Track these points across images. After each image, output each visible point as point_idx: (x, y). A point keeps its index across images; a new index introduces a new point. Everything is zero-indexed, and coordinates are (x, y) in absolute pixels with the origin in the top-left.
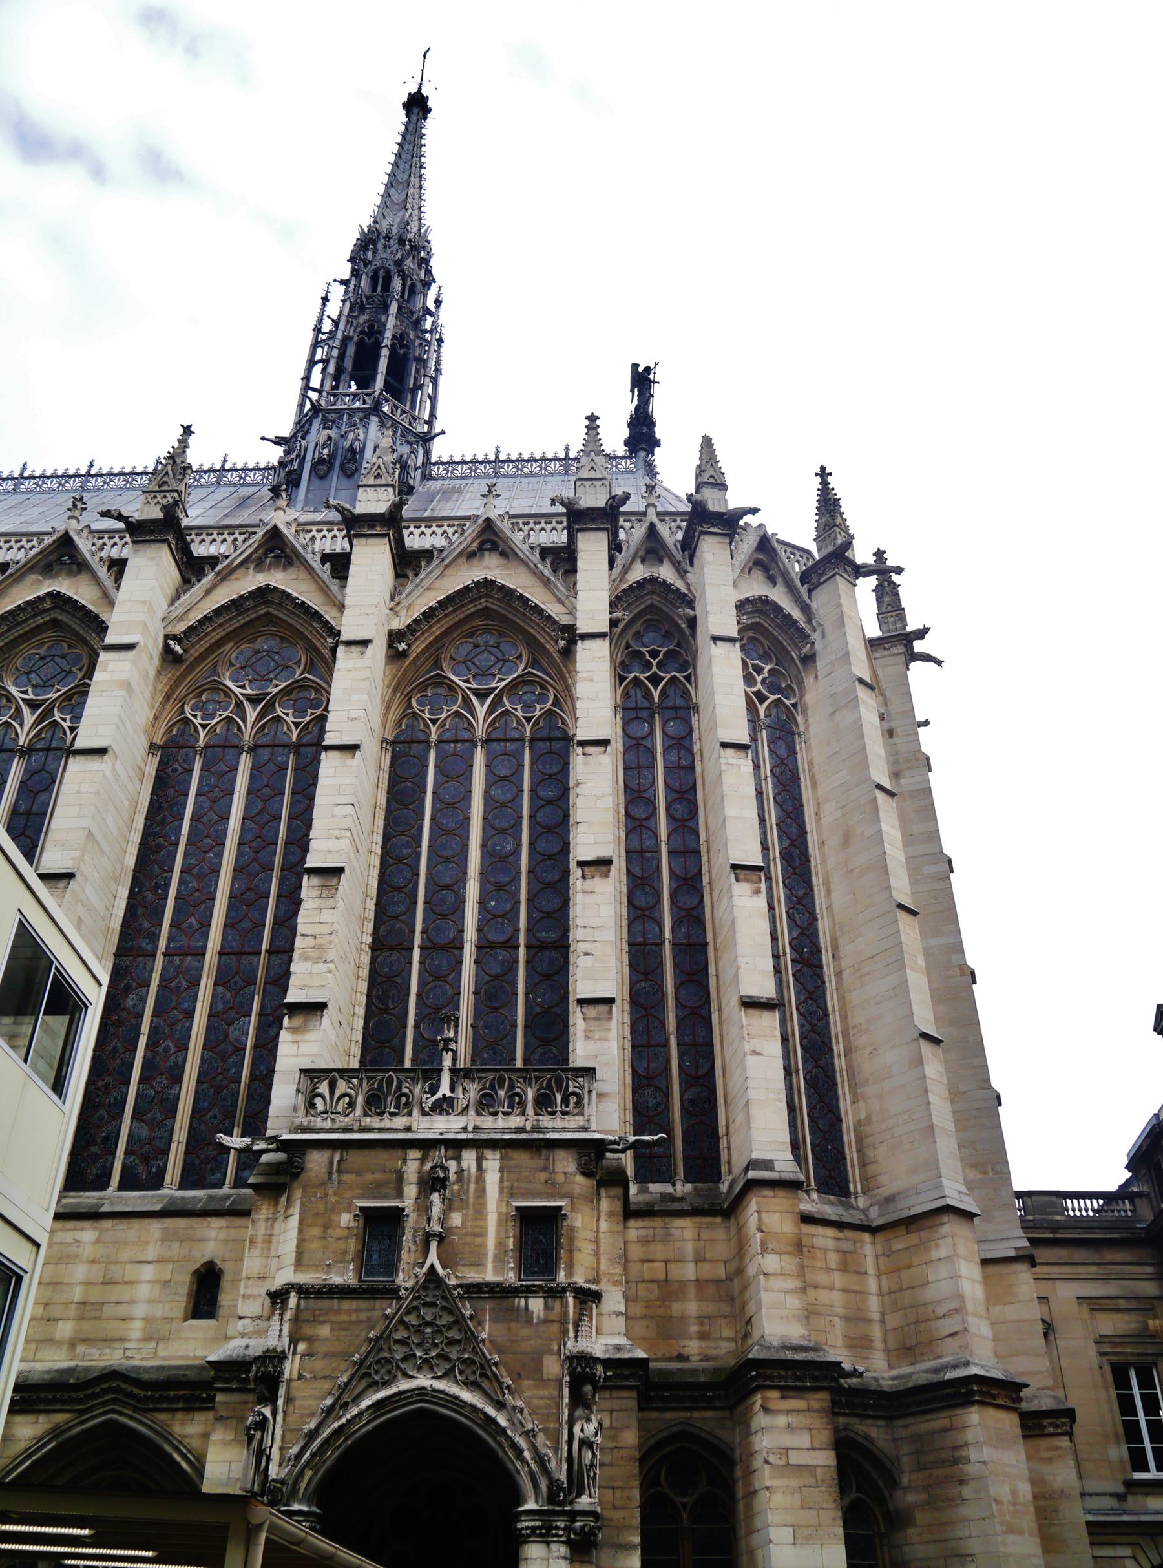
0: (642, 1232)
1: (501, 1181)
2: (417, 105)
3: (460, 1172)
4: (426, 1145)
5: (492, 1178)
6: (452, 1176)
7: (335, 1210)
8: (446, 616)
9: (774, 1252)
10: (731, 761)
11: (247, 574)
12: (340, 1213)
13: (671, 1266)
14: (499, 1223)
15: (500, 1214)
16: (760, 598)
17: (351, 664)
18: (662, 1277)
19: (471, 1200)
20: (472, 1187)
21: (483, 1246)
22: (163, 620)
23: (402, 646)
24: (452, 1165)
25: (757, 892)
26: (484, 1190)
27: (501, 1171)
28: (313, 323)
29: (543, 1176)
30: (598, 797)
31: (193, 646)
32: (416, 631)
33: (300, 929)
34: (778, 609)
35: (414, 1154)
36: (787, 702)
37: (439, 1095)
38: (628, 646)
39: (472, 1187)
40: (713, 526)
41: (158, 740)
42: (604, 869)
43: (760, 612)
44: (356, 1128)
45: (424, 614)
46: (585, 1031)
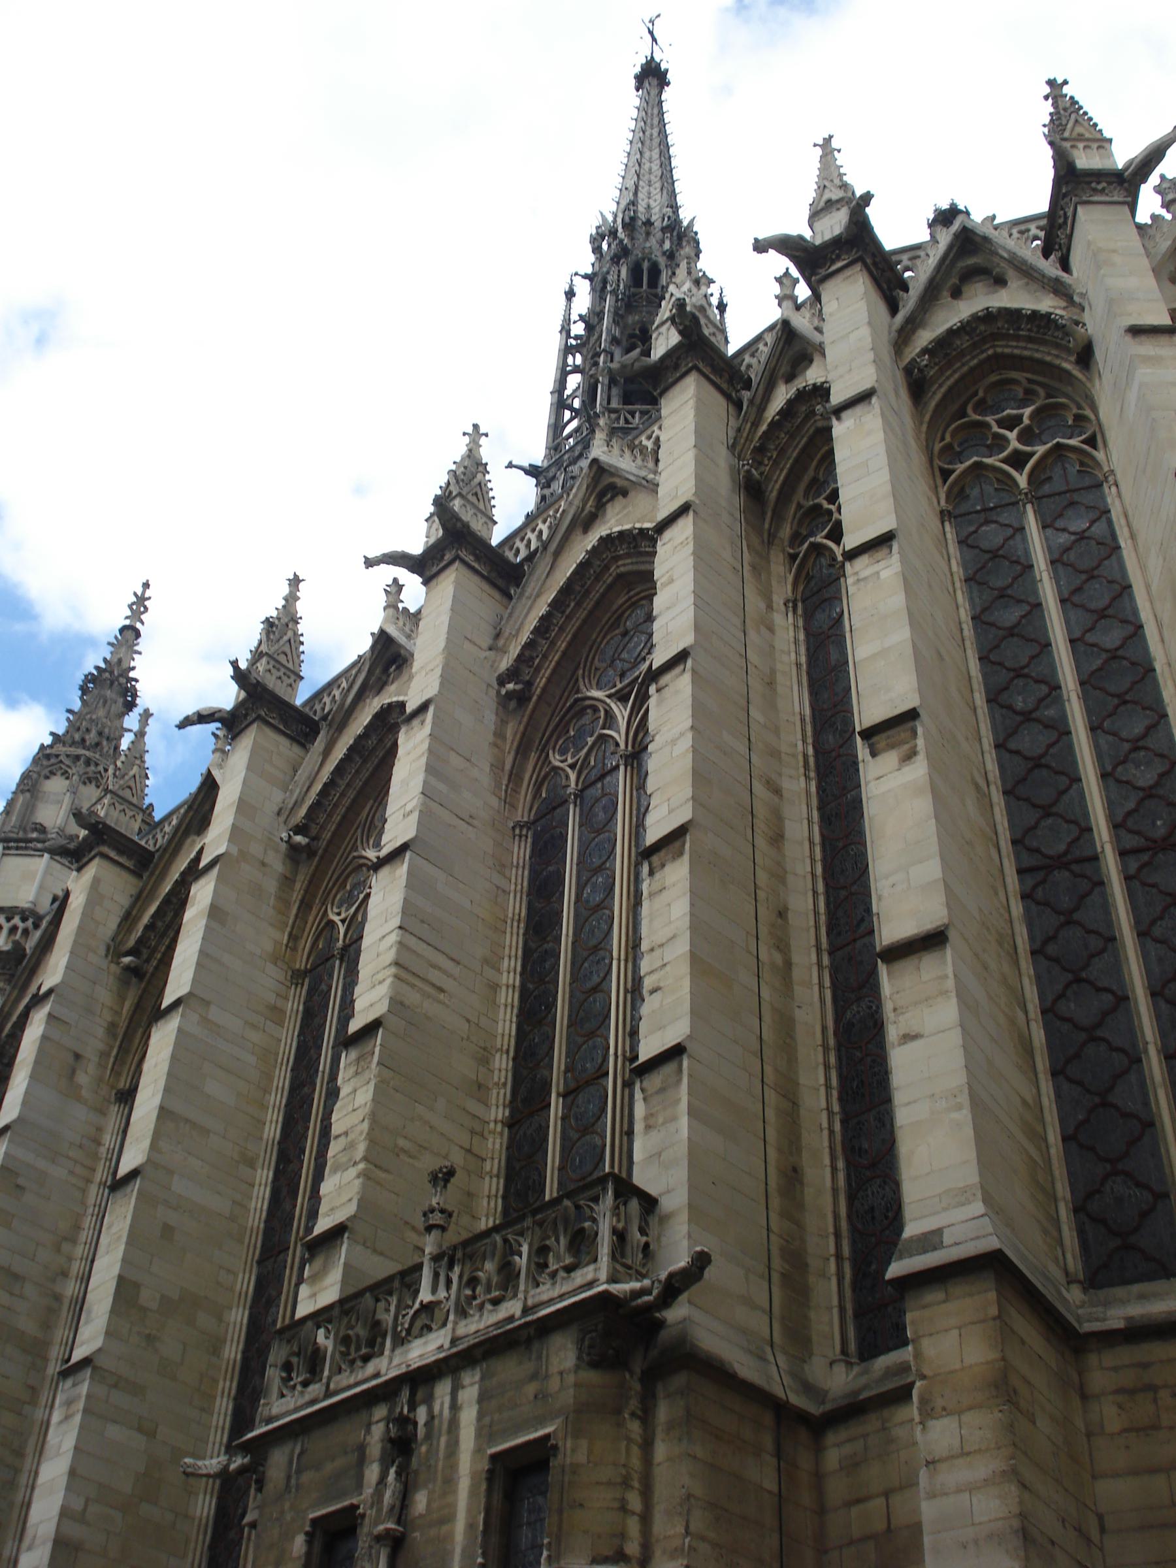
0: (847, 1449)
1: (481, 1416)
2: (652, 76)
3: (429, 1423)
4: (386, 1392)
5: (468, 1416)
6: (421, 1431)
7: (288, 1537)
8: (569, 618)
9: (946, 1412)
10: (864, 574)
11: (364, 707)
12: (293, 1538)
13: (896, 1500)
14: (473, 1493)
15: (474, 1475)
16: (975, 318)
17: (410, 745)
18: (880, 1526)
19: (441, 1463)
20: (443, 1440)
21: (450, 1536)
22: (279, 814)
23: (510, 686)
24: (421, 1414)
25: (910, 756)
26: (457, 1442)
27: (480, 1401)
28: (550, 384)
29: (531, 1389)
30: (674, 742)
31: (323, 828)
32: (532, 659)
33: (336, 1129)
34: (1013, 315)
35: (380, 1412)
36: (1073, 442)
37: (417, 1306)
38: (799, 506)
39: (443, 1440)
40: (833, 262)
41: (301, 963)
42: (677, 844)
43: (995, 337)
44: (321, 1396)
45: (536, 631)
46: (646, 1118)
